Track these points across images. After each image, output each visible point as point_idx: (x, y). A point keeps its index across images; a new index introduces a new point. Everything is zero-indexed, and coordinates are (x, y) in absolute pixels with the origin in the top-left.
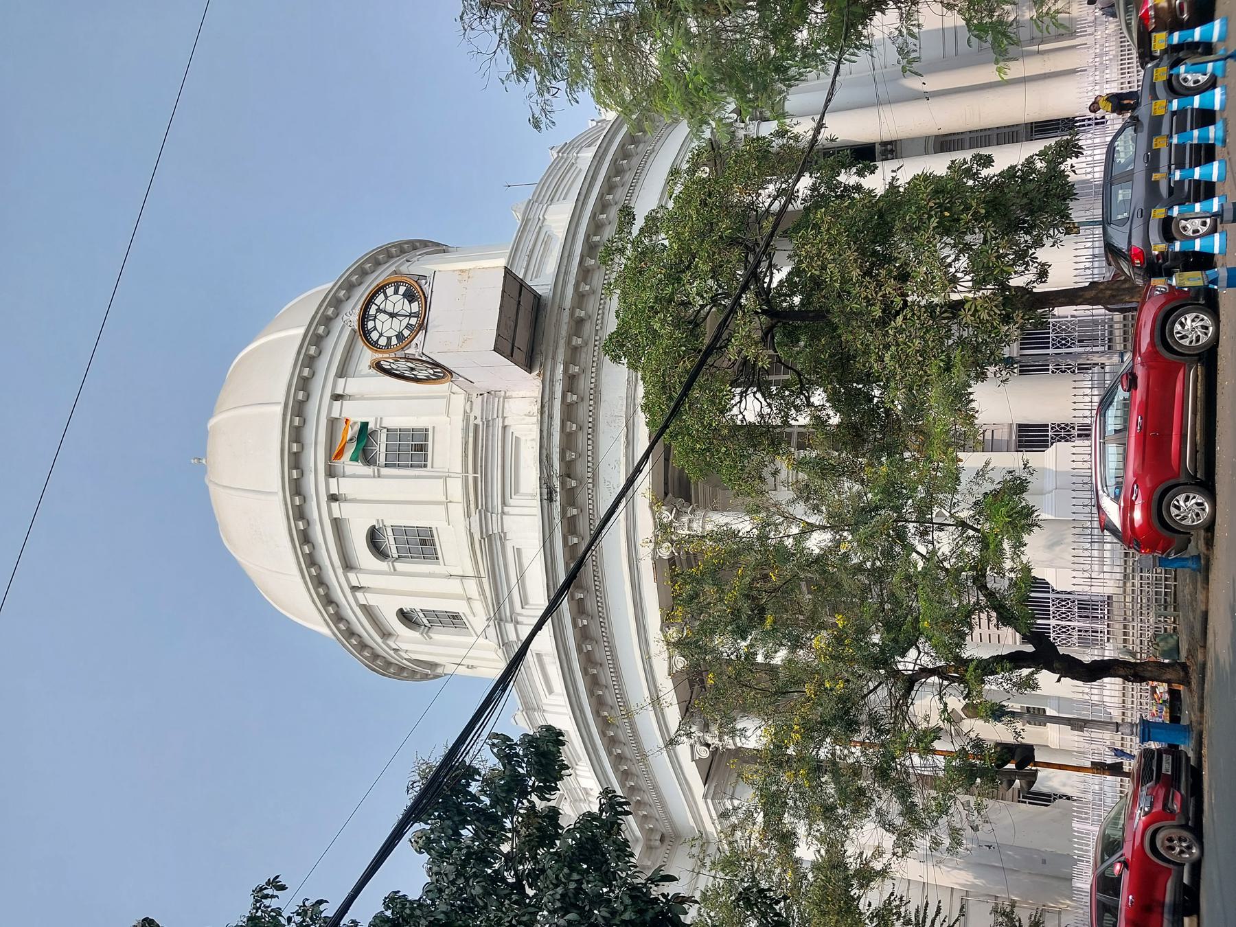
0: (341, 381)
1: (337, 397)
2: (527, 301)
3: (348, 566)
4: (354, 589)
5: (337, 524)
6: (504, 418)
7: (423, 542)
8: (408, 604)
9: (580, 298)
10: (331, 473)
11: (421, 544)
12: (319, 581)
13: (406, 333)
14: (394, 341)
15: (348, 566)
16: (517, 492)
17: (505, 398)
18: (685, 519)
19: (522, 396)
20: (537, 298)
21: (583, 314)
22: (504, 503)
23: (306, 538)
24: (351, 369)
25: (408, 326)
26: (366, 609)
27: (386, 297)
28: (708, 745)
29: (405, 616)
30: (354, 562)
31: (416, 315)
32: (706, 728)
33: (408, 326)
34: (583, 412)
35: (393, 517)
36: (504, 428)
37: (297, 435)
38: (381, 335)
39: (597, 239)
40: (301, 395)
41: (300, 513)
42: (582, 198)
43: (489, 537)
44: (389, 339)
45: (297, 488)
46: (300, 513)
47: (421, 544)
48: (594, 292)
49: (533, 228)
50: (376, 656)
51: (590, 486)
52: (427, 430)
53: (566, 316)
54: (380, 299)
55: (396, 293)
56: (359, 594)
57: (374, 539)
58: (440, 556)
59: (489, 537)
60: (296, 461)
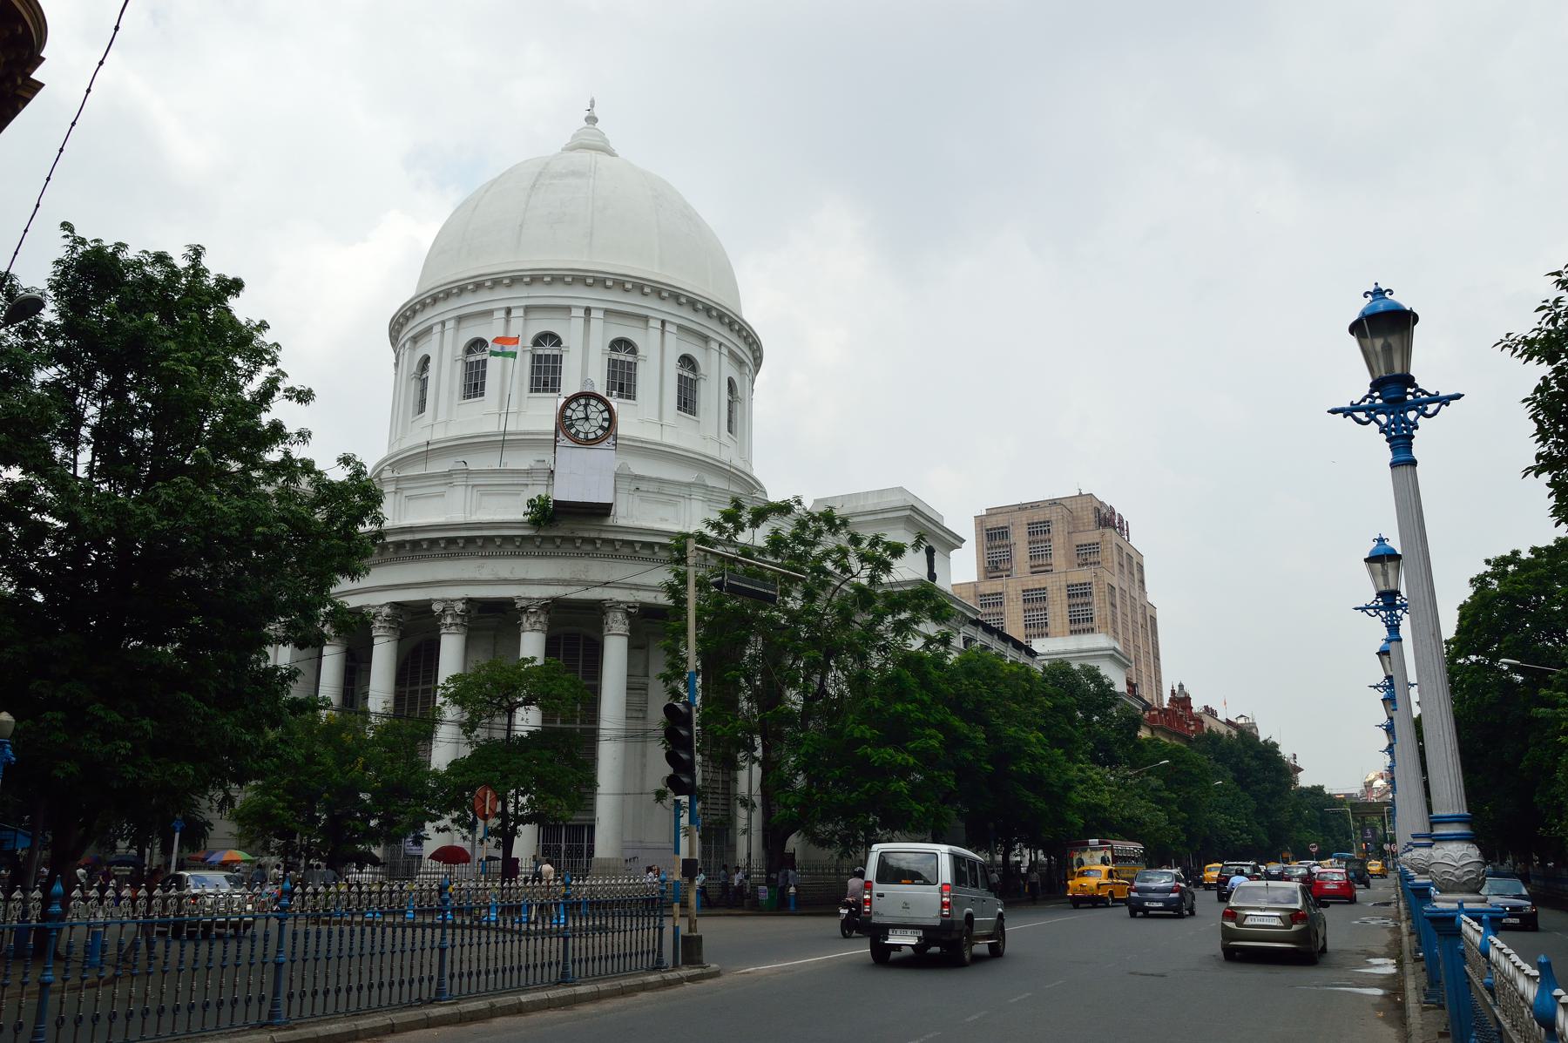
0: (600, 315)
1: (588, 310)
3: (460, 319)
4: (443, 323)
5: (490, 313)
8: (432, 365)
11: (474, 385)
12: (448, 294)
15: (460, 319)
18: (458, 621)
23: (479, 286)
24: (614, 320)
25: (578, 432)
26: (429, 330)
29: (426, 359)
30: (464, 324)
33: (578, 432)
37: (557, 279)
40: (590, 281)
41: (496, 282)
45: (515, 280)
46: (496, 282)
47: (474, 385)
49: (685, 491)
50: (407, 319)
53: (593, 535)
54: (601, 407)
60: (535, 279)
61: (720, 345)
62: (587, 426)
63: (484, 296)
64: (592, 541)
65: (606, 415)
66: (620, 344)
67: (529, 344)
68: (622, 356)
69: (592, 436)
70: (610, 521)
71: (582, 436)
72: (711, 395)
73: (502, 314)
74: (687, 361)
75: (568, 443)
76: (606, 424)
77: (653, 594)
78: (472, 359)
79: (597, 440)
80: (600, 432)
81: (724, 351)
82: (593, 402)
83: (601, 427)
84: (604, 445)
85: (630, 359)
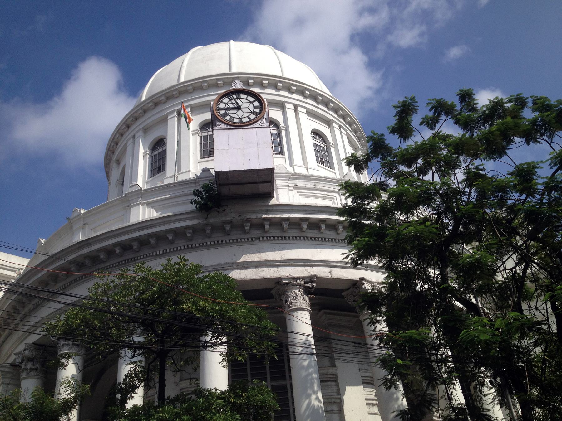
2: (262, 188)
4: (134, 137)
9: (278, 224)
13: (228, 118)
20: (270, 195)
21: (267, 227)
27: (252, 102)
32: (30, 359)
38: (226, 104)
39: (323, 227)
48: (282, 229)
51: (154, 254)
54: (251, 99)
55: (255, 107)
56: (131, 140)
62: (240, 113)
65: (256, 104)
70: (273, 202)
76: (258, 110)
77: (327, 270)
78: (156, 153)
79: (251, 123)
80: (252, 117)
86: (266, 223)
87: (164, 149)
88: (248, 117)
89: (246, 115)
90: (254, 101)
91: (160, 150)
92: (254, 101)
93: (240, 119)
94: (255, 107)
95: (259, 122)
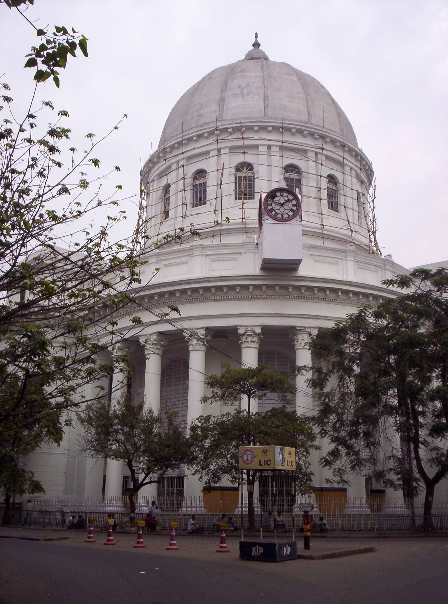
0: (277, 149)
4: (178, 162)
5: (208, 153)
6: (245, 253)
7: (200, 200)
9: (298, 288)
10: (231, 148)
11: (200, 197)
13: (273, 213)
14: (270, 207)
16: (213, 261)
17: (255, 253)
19: (247, 266)
21: (290, 290)
22: (207, 255)
24: (285, 153)
28: (113, 350)
31: (282, 217)
34: (244, 293)
35: (212, 180)
36: (241, 253)
42: (348, 283)
43: (191, 249)
44: (271, 205)
47: (200, 197)
52: (254, 198)
55: (293, 205)
57: (201, 173)
58: (195, 208)
59: (191, 249)
61: (351, 168)
62: (282, 209)
63: (202, 143)
64: (286, 287)
66: (290, 168)
67: (233, 170)
68: (292, 175)
69: (285, 216)
71: (279, 216)
72: (347, 199)
73: (215, 153)
74: (331, 178)
75: (270, 220)
76: (294, 208)
78: (197, 182)
79: (290, 218)
80: (291, 213)
81: (354, 173)
82: (285, 194)
83: (292, 210)
84: (294, 221)
85: (296, 177)
86: (290, 287)
87: (205, 181)
88: (287, 213)
89: (286, 212)
90: (292, 200)
91: (201, 181)
92: (292, 200)
93: (282, 214)
94: (293, 205)
95: (295, 219)
